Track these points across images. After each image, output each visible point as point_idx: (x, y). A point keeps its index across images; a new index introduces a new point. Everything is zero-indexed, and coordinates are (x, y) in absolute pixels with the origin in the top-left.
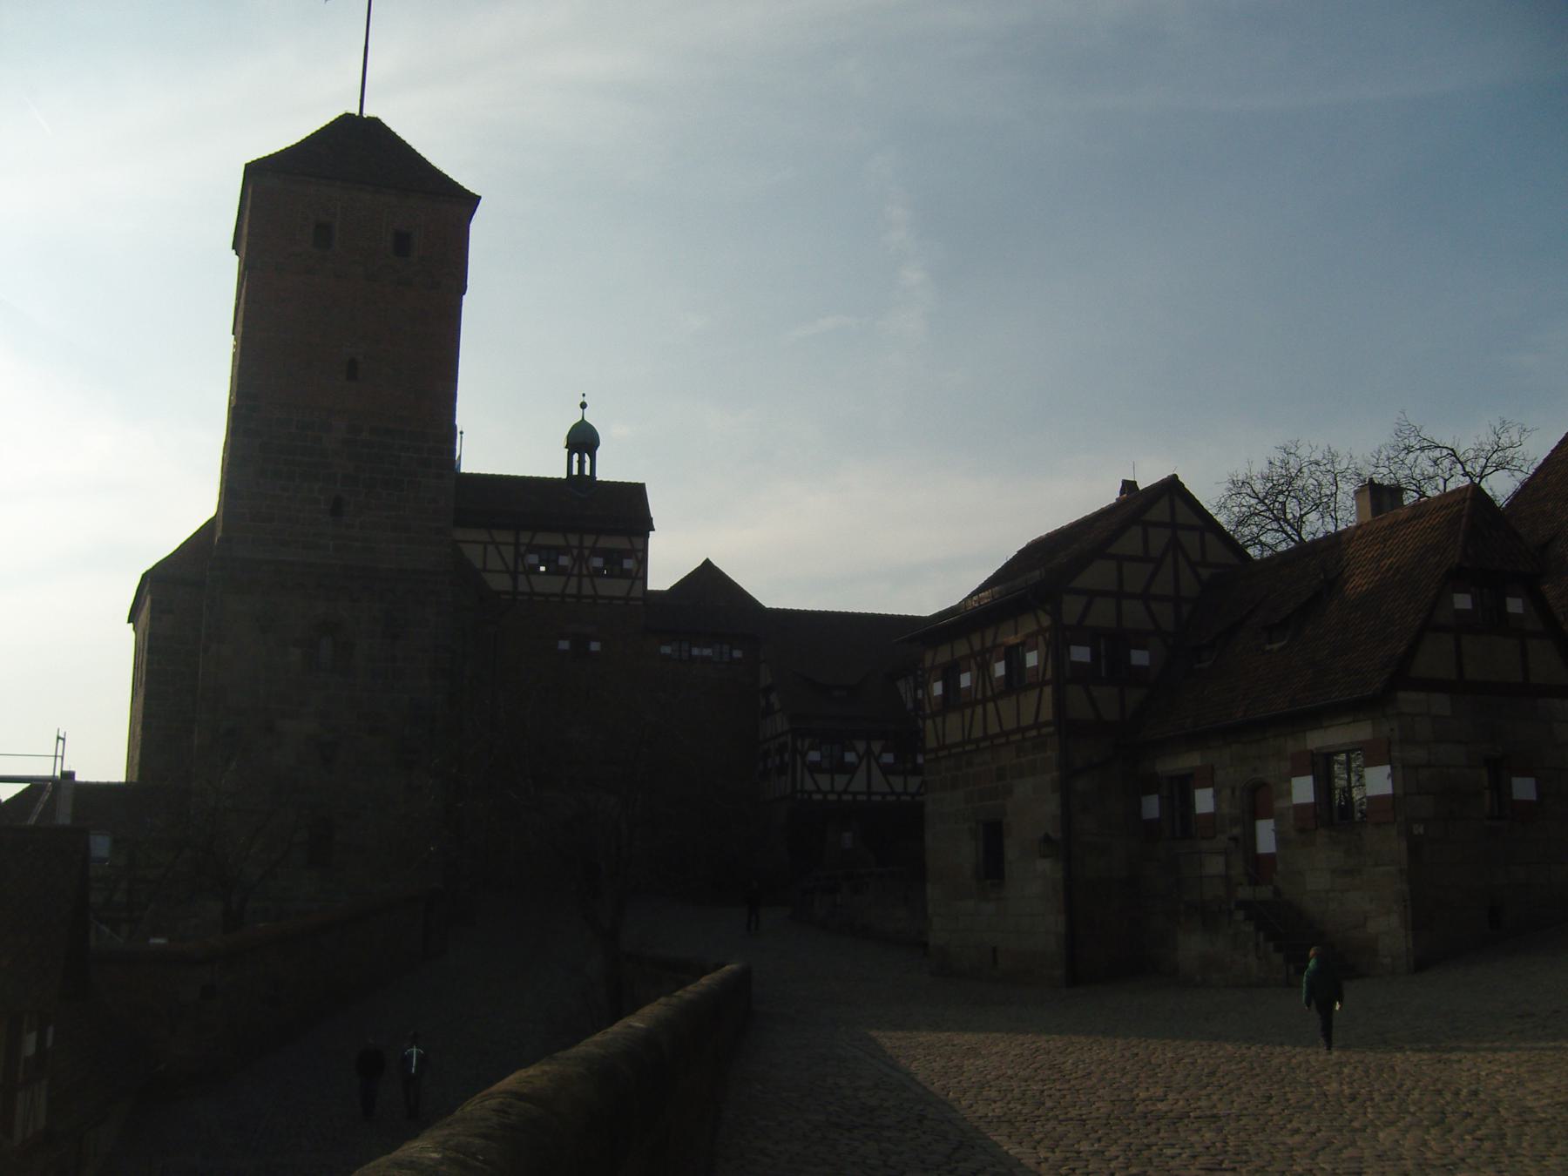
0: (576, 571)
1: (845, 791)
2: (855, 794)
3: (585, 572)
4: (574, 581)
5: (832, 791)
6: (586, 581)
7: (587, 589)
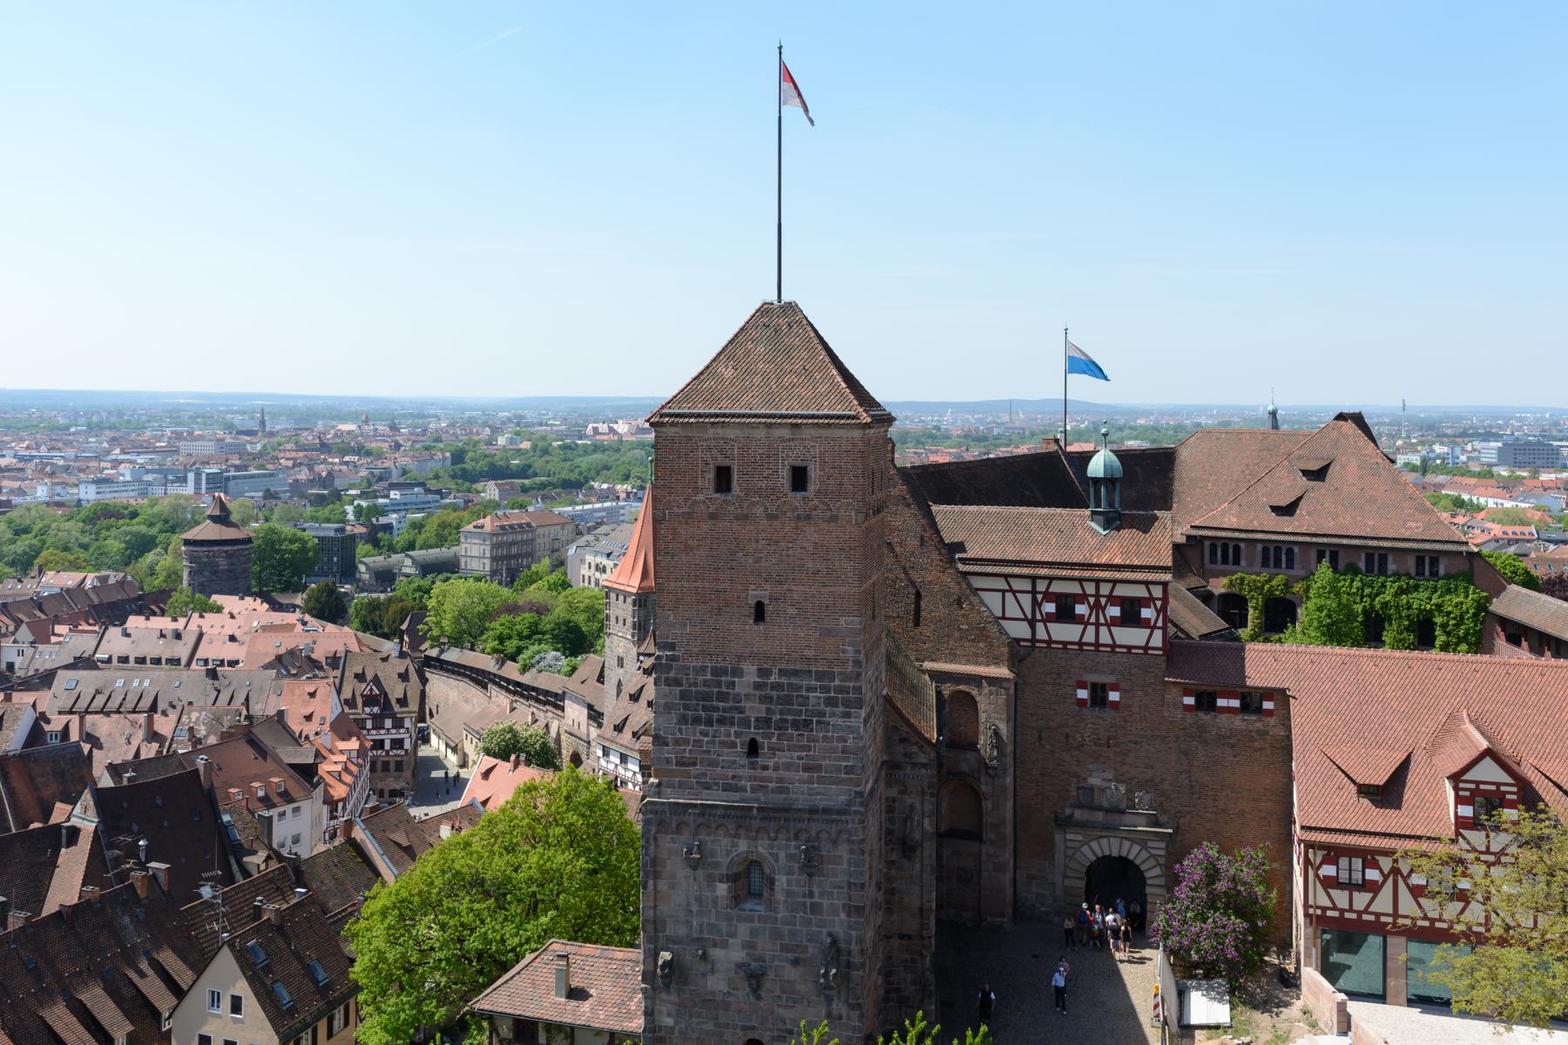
0: (1093, 620)
1: (1366, 911)
2: (1378, 915)
3: (1102, 620)
4: (1091, 629)
5: (1351, 910)
6: (1103, 630)
7: (1105, 638)
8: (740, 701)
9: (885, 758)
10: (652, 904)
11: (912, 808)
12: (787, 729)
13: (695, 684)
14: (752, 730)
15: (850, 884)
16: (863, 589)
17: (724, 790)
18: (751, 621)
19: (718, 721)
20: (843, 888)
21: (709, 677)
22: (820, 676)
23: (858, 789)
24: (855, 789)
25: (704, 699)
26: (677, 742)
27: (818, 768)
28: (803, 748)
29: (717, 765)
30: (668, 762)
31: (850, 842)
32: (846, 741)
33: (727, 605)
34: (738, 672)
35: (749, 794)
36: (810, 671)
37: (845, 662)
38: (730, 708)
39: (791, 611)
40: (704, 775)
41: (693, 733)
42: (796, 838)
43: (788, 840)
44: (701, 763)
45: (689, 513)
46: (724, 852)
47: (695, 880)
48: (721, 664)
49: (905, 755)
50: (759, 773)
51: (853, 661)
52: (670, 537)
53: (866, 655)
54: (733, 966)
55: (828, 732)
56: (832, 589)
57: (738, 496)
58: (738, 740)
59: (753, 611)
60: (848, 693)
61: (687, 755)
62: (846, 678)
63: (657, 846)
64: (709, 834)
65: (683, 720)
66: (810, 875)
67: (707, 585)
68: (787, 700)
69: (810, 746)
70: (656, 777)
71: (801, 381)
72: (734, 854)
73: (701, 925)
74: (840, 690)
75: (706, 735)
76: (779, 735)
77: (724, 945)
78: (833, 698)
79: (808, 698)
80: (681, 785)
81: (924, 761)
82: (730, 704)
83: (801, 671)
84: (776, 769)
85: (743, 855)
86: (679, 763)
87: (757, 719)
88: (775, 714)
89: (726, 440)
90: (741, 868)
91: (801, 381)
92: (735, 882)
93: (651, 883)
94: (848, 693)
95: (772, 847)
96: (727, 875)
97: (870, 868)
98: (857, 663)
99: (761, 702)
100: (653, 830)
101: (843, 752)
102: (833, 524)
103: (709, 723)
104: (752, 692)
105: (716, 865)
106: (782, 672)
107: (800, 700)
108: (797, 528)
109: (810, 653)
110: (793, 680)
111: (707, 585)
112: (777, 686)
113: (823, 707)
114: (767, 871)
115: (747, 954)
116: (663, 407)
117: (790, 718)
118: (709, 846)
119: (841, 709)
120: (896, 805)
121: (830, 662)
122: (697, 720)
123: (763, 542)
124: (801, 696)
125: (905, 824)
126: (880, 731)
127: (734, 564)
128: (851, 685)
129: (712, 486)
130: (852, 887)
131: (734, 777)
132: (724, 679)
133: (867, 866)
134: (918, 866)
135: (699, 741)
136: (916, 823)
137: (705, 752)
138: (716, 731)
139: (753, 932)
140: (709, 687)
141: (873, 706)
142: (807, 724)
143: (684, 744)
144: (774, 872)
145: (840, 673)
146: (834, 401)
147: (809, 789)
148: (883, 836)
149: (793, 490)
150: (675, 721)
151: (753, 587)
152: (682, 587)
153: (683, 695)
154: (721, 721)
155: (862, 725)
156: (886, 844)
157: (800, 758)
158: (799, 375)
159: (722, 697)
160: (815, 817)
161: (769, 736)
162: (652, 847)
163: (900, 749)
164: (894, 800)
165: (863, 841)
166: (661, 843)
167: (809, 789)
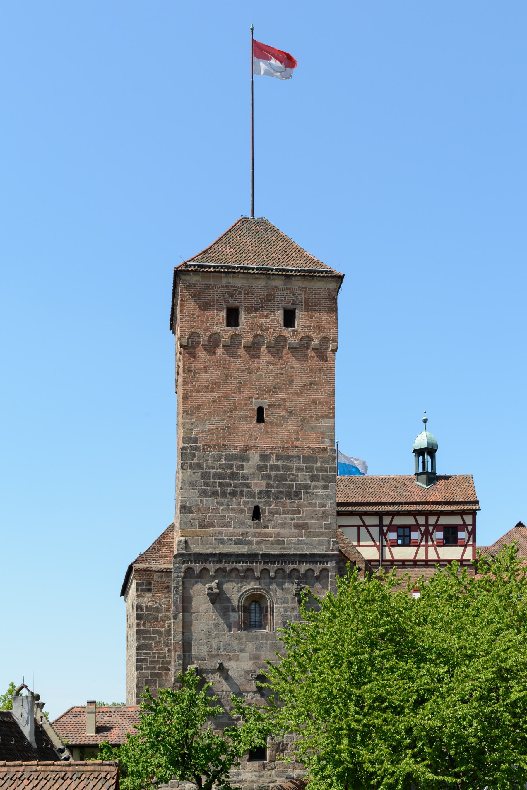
10: (181, 630)
12: (282, 498)
13: (213, 467)
14: (257, 500)
17: (236, 543)
19: (230, 494)
22: (306, 459)
27: (304, 526)
28: (294, 512)
29: (230, 526)
34: (245, 458)
35: (255, 546)
37: (324, 450)
39: (285, 414)
40: (221, 533)
41: (210, 502)
44: (218, 525)
54: (243, 673)
59: (255, 413)
61: (208, 520)
65: (204, 493)
67: (221, 395)
68: (283, 478)
72: (244, 591)
73: (218, 645)
74: (321, 469)
75: (221, 504)
77: (237, 658)
78: (315, 475)
79: (297, 476)
83: (292, 456)
86: (201, 526)
87: (260, 492)
88: (272, 487)
89: (236, 288)
99: (263, 478)
101: (323, 513)
103: (224, 495)
106: (278, 458)
107: (292, 477)
109: (298, 444)
111: (221, 395)
112: (272, 468)
113: (308, 482)
115: (254, 663)
119: (322, 483)
121: (313, 450)
122: (215, 494)
124: (293, 475)
129: (225, 322)
131: (243, 534)
132: (235, 463)
137: (221, 516)
139: (258, 648)
140: (223, 469)
142: (297, 494)
145: (320, 457)
153: (204, 475)
154: (233, 494)
157: (292, 519)
159: (233, 476)
160: (304, 560)
161: (268, 504)
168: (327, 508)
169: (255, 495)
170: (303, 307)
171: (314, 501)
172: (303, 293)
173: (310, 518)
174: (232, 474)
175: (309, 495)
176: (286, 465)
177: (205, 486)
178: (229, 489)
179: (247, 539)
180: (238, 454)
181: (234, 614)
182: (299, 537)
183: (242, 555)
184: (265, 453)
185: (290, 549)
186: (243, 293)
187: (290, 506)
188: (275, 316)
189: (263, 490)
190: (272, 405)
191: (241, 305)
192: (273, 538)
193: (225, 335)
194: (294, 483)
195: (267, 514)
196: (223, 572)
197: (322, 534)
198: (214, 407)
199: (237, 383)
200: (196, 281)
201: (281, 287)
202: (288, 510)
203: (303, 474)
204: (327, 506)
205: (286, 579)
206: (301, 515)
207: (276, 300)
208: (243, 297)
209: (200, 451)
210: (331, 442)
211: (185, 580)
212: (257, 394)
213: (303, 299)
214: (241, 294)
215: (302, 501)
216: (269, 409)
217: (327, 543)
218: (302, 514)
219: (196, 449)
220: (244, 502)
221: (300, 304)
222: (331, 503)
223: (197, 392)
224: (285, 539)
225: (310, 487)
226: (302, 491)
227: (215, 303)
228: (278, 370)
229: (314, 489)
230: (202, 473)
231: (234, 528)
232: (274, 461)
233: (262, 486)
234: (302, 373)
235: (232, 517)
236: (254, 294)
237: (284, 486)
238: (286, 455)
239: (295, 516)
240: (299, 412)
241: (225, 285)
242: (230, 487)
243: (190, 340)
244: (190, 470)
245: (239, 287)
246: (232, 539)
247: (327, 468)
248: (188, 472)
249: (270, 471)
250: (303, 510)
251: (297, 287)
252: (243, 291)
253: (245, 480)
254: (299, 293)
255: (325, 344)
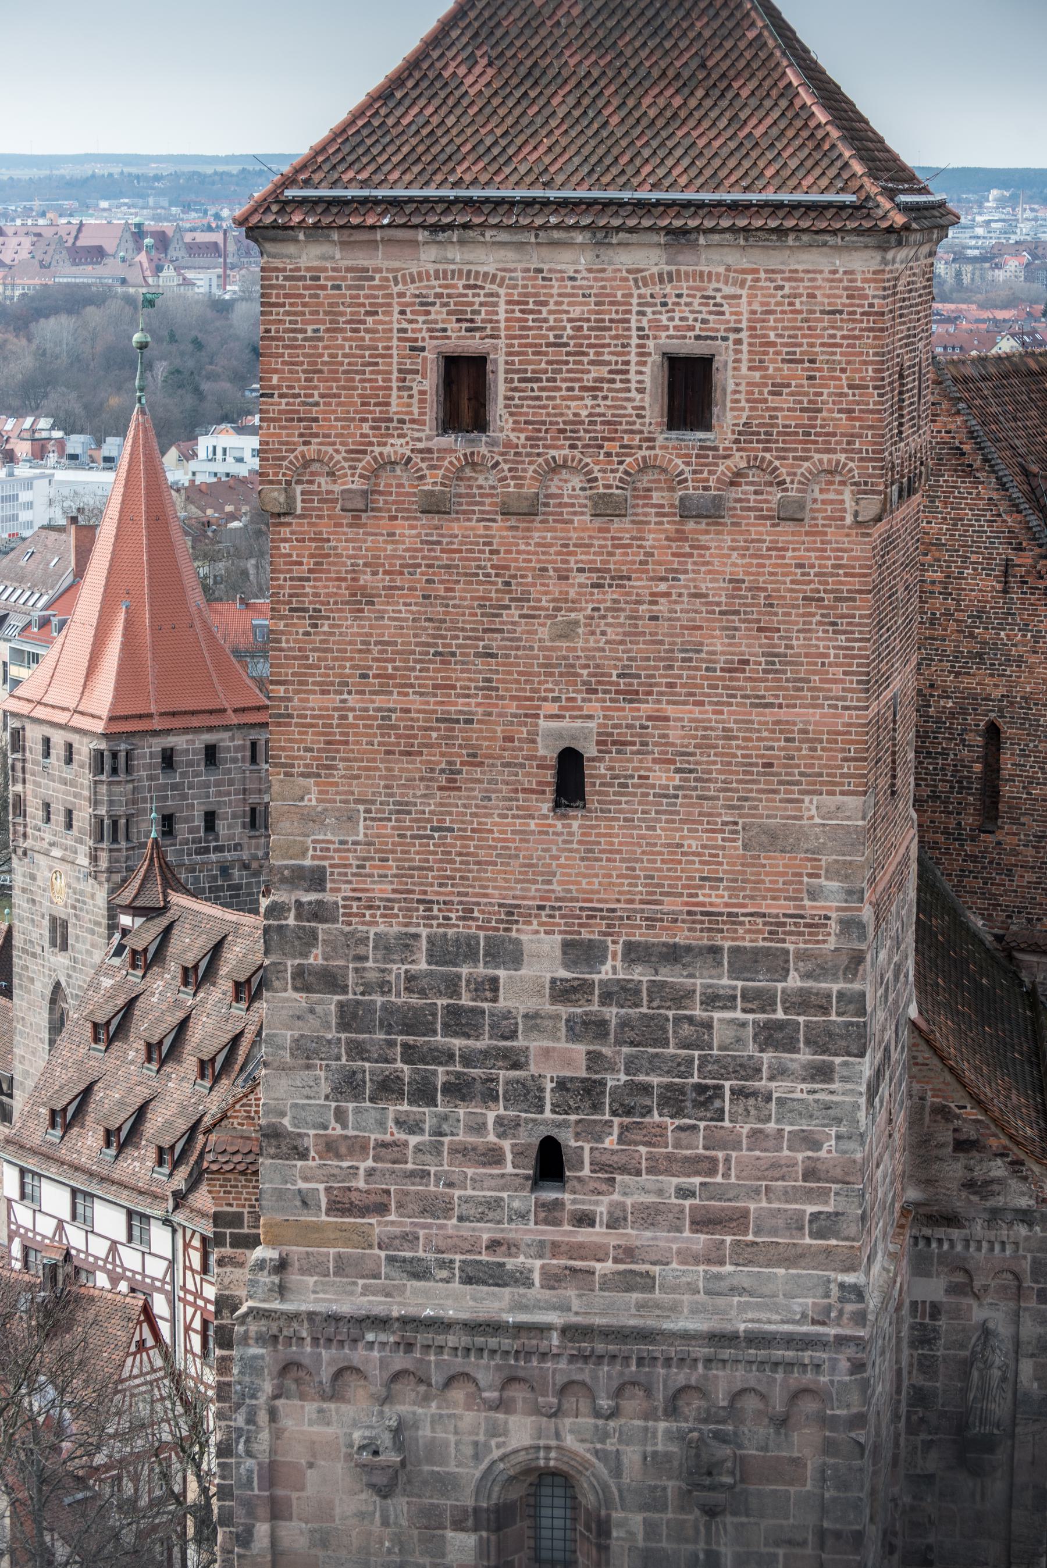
8: (513, 1035)
9: (913, 1194)
11: (986, 1333)
12: (649, 1111)
13: (383, 987)
14: (548, 1114)
15: (822, 1534)
16: (871, 713)
17: (468, 1280)
18: (546, 807)
20: (803, 1544)
21: (423, 966)
23: (850, 1278)
24: (843, 1277)
25: (409, 1029)
26: (330, 1148)
27: (737, 1221)
29: (447, 1211)
30: (305, 1203)
31: (825, 1421)
32: (816, 1146)
33: (474, 759)
35: (537, 1292)
36: (715, 950)
37: (817, 925)
38: (486, 1053)
39: (662, 777)
40: (410, 1239)
42: (672, 1410)
43: (649, 1415)
44: (400, 1206)
45: (364, 493)
46: (469, 1451)
47: (385, 1523)
48: (458, 929)
49: (970, 1185)
50: (566, 1233)
51: (841, 921)
52: (308, 563)
53: (876, 905)
55: (768, 1119)
56: (783, 714)
57: (508, 444)
58: (507, 1145)
59: (550, 776)
60: (825, 1010)
61: (361, 1184)
62: (820, 970)
63: (277, 1435)
64: (426, 1399)
66: (711, 1512)
67: (414, 701)
69: (714, 1160)
70: (272, 1243)
71: (693, 103)
72: (496, 1454)
74: (802, 1002)
75: (415, 1128)
76: (624, 1129)
78: (780, 1025)
79: (708, 1026)
80: (342, 1266)
81: (1024, 1202)
82: (484, 1043)
83: (689, 949)
84: (615, 1222)
85: (522, 1457)
86: (336, 1207)
87: (562, 1085)
88: (612, 1069)
90: (515, 1494)
91: (693, 103)
92: (498, 1529)
93: (262, 1529)
94: (825, 1010)
95: (604, 1436)
96: (476, 1510)
97: (873, 1492)
98: (851, 926)
99: (573, 1035)
100: (268, 1387)
101: (810, 1174)
102: (789, 527)
103: (424, 1094)
104: (549, 1008)
105: (445, 1484)
106: (634, 953)
107: (686, 1029)
108: (681, 536)
109: (716, 899)
110: (669, 975)
111: (414, 701)
113: (751, 1049)
114: (589, 1500)
116: (288, 181)
117: (655, 1080)
118: (425, 1432)
119: (805, 1056)
120: (942, 1323)
121: (776, 927)
123: (582, 578)
124: (690, 1019)
125: (966, 1376)
126: (901, 1119)
127: (496, 642)
128: (835, 987)
129: (431, 413)
130: (830, 1542)
131: (494, 1245)
132: (465, 970)
133: (867, 1486)
134: (998, 1487)
135: (395, 1144)
136: (996, 1373)
137: (412, 1174)
138: (445, 1118)
140: (423, 993)
141: (887, 1050)
143: (351, 1153)
144: (608, 1503)
145: (802, 956)
146: (793, 164)
147: (709, 1278)
148: (903, 1408)
149: (672, 425)
150: (325, 1088)
151: (552, 708)
152: (343, 709)
154: (458, 1090)
155: (863, 1101)
156: (911, 1430)
157: (684, 1193)
158: (686, 87)
160: (726, 1353)
162: (264, 1436)
163: (954, 1170)
164: (935, 1310)
165: (858, 1421)
166: (287, 1422)
167: (709, 1278)
168: (823, 1154)
169: (541, 1099)
170: (745, 348)
171: (772, 1126)
172: (744, 292)
173: (757, 1191)
174: (454, 1012)
175: (751, 1101)
176: (663, 984)
177: (351, 1058)
178: (441, 1069)
179: (511, 1263)
180: (477, 938)
181: (461, 1536)
182: (709, 1261)
183: (495, 1328)
184: (585, 935)
185: (674, 1308)
186: (502, 301)
187: (677, 1146)
188: (629, 390)
189: (572, 1079)
190: (614, 743)
191: (495, 348)
192: (609, 1263)
193: (432, 467)
194: (696, 1053)
195: (586, 1171)
196: (421, 1381)
197: (802, 1256)
198: (388, 752)
199: (477, 655)
200: (324, 258)
201: (655, 270)
202: (670, 1158)
203: (733, 1021)
204: (825, 1146)
205: (657, 1419)
206: (719, 1179)
207: (634, 325)
208: (502, 316)
209: (335, 920)
210: (850, 892)
211: (280, 1403)
212: (556, 700)
213: (745, 317)
214: (495, 304)
215: (727, 1124)
216: (601, 760)
217: (820, 1291)
218: (726, 1175)
219: (320, 913)
220: (499, 1121)
221: (732, 336)
222: (838, 1137)
223: (323, 692)
224: (657, 1269)
225: (759, 1070)
226: (727, 1084)
227: (395, 343)
228: (639, 602)
229: (771, 1078)
230: (341, 1005)
231: (461, 1219)
232: (619, 964)
233: (569, 1063)
234: (737, 613)
235: (455, 1178)
236: (545, 304)
237: (654, 1064)
238: (665, 944)
239: (697, 1180)
240: (720, 772)
241: (431, 268)
242: (446, 1064)
243: (299, 489)
244: (297, 995)
245: (486, 274)
246: (452, 1262)
247: (829, 996)
248: (287, 1000)
249: (602, 1004)
250: (727, 1160)
251: (721, 269)
252: (502, 291)
253: (505, 1038)
254: (728, 290)
255: (832, 496)
